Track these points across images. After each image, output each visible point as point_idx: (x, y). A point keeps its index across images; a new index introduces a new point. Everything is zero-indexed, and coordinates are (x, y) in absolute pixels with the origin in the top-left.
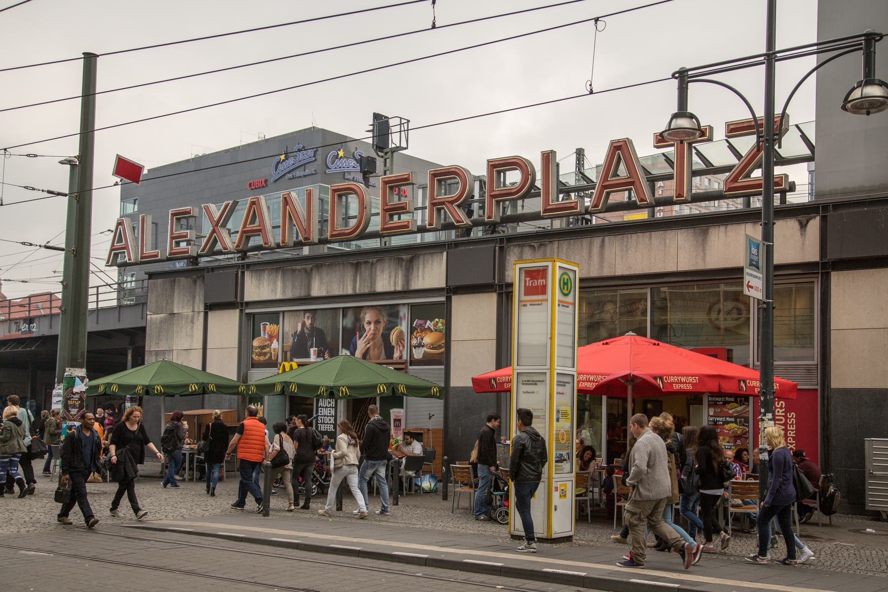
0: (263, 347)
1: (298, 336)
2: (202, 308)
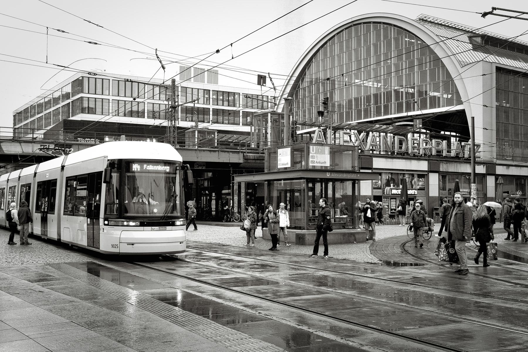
0: (376, 183)
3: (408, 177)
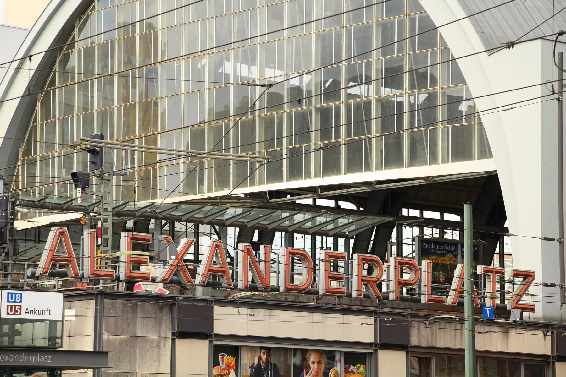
1: (255, 368)
2: (169, 335)
3: (316, 360)
